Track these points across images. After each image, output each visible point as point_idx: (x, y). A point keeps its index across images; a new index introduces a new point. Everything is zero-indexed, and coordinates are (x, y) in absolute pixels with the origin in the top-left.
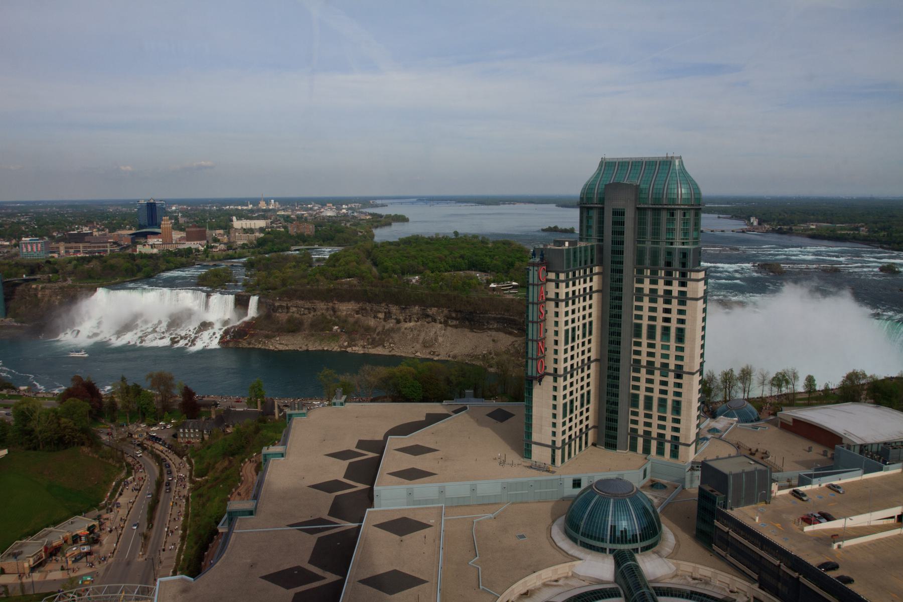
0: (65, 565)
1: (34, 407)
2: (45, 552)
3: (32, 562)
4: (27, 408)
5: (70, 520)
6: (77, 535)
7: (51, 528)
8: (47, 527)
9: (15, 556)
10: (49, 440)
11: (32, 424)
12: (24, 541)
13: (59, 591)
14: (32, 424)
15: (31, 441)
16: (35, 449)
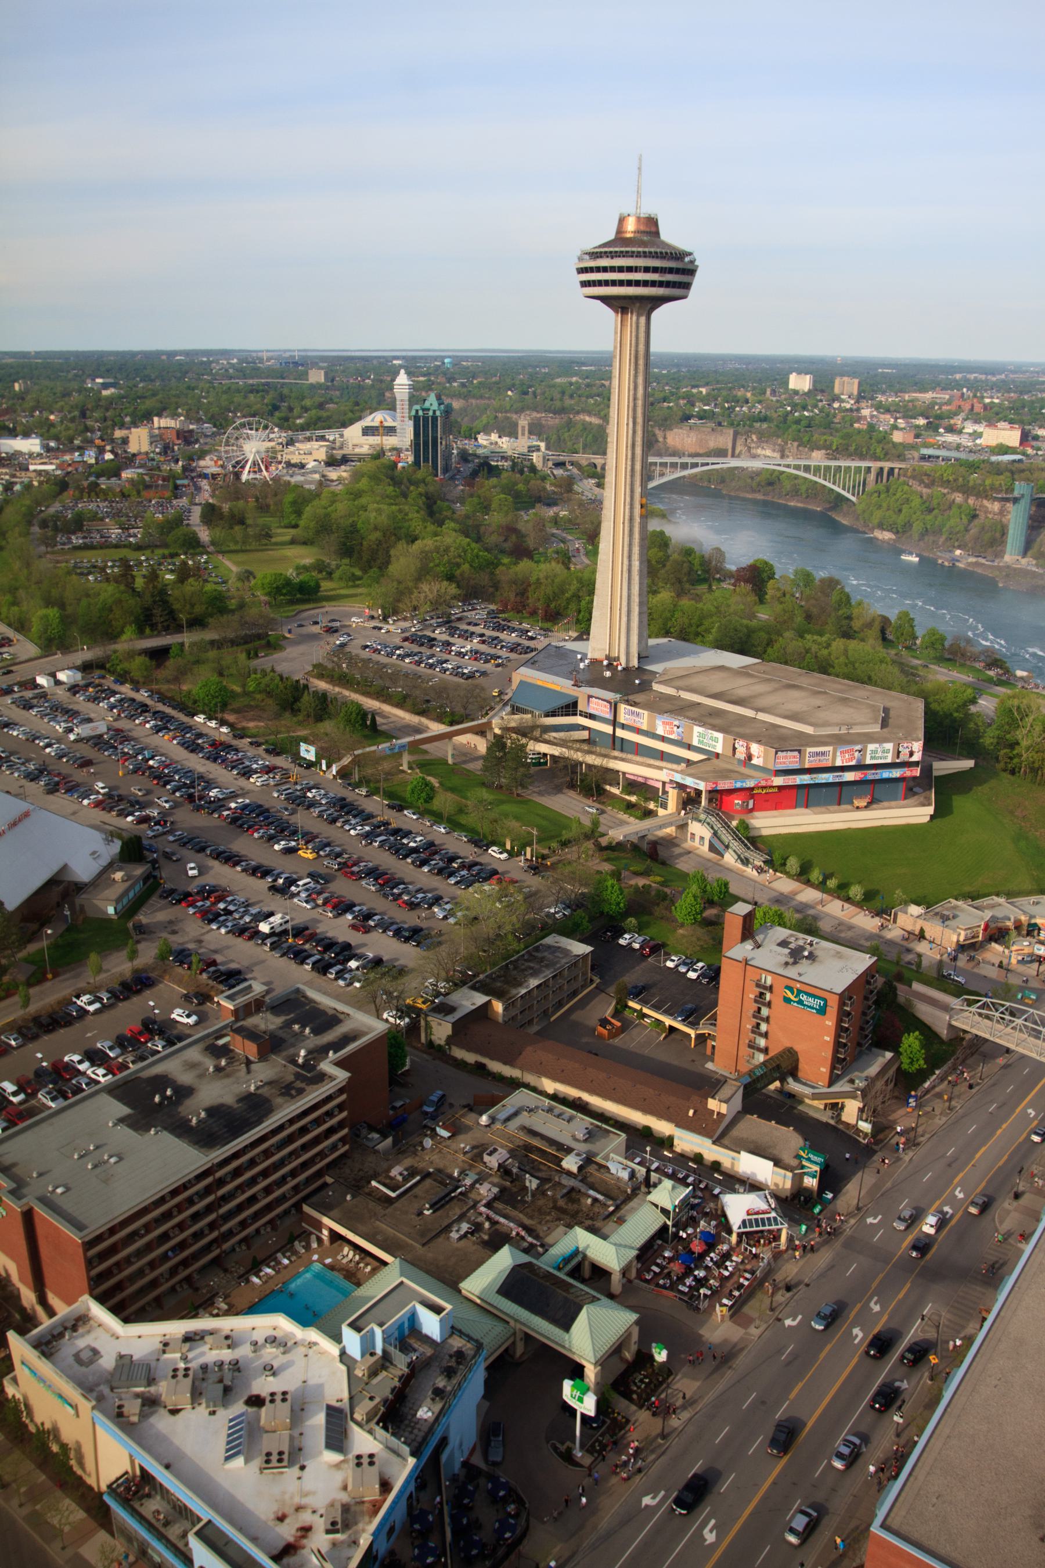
0: (1005, 961)
1: (1029, 707)
2: (985, 929)
3: (962, 938)
4: (1018, 708)
5: (1033, 899)
6: (1035, 925)
7: (1001, 900)
8: (997, 895)
9: (945, 919)
10: (1036, 765)
11: (1019, 734)
12: (960, 903)
13: (986, 996)
14: (1019, 734)
15: (1011, 758)
16: (1013, 772)
